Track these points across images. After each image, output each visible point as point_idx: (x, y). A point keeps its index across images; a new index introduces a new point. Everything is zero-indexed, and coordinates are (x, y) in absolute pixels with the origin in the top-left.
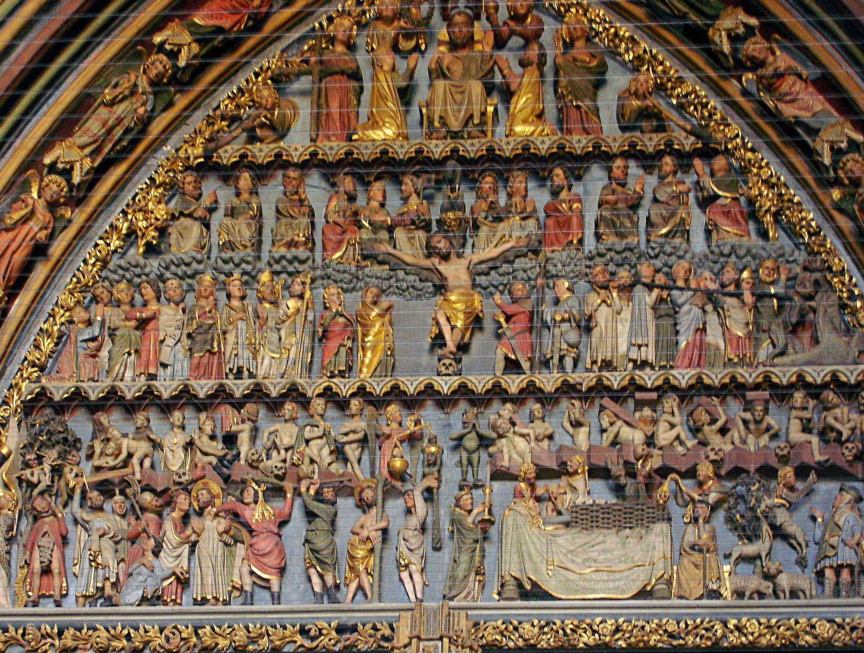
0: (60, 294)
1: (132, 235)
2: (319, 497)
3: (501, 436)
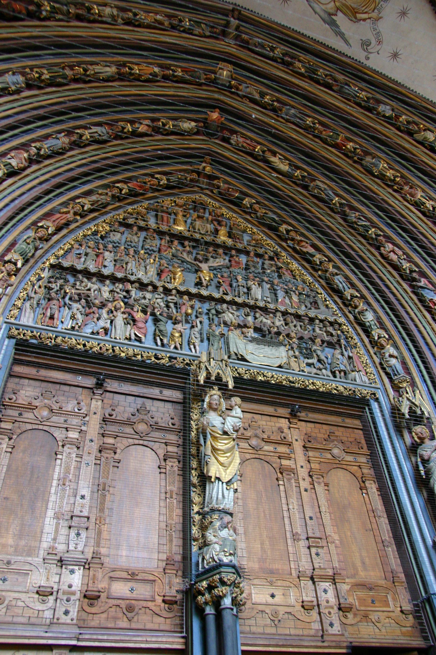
0: (70, 239)
1: (95, 233)
3: (224, 312)
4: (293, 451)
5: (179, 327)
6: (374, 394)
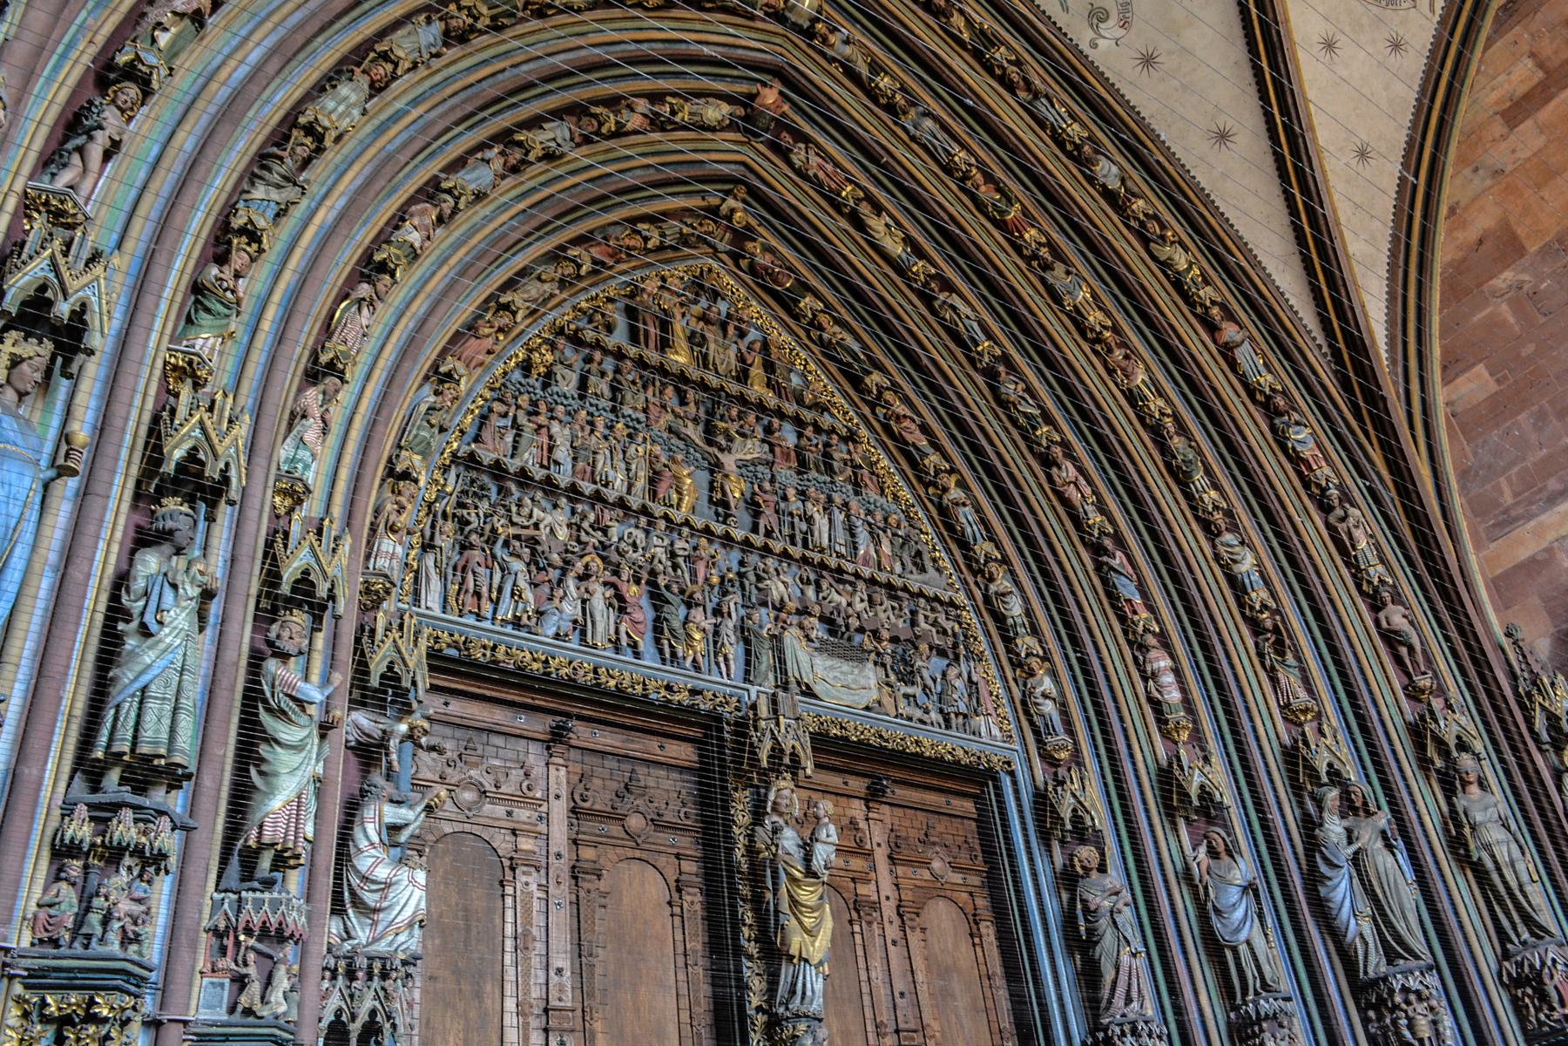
2: (667, 587)
5: (697, 614)
6: (1009, 763)
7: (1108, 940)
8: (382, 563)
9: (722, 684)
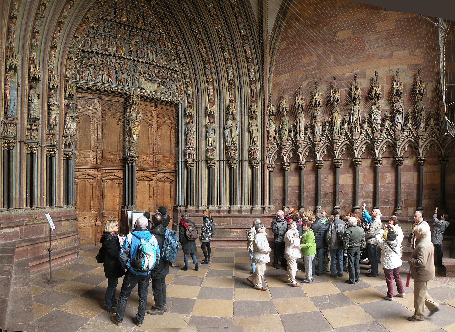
4: (154, 119)
5: (124, 75)
7: (189, 134)
8: (68, 75)
9: (128, 87)
